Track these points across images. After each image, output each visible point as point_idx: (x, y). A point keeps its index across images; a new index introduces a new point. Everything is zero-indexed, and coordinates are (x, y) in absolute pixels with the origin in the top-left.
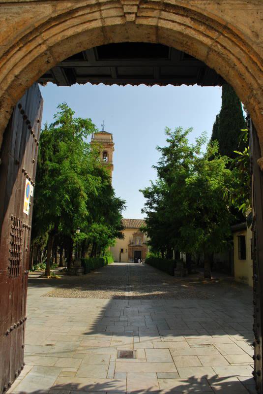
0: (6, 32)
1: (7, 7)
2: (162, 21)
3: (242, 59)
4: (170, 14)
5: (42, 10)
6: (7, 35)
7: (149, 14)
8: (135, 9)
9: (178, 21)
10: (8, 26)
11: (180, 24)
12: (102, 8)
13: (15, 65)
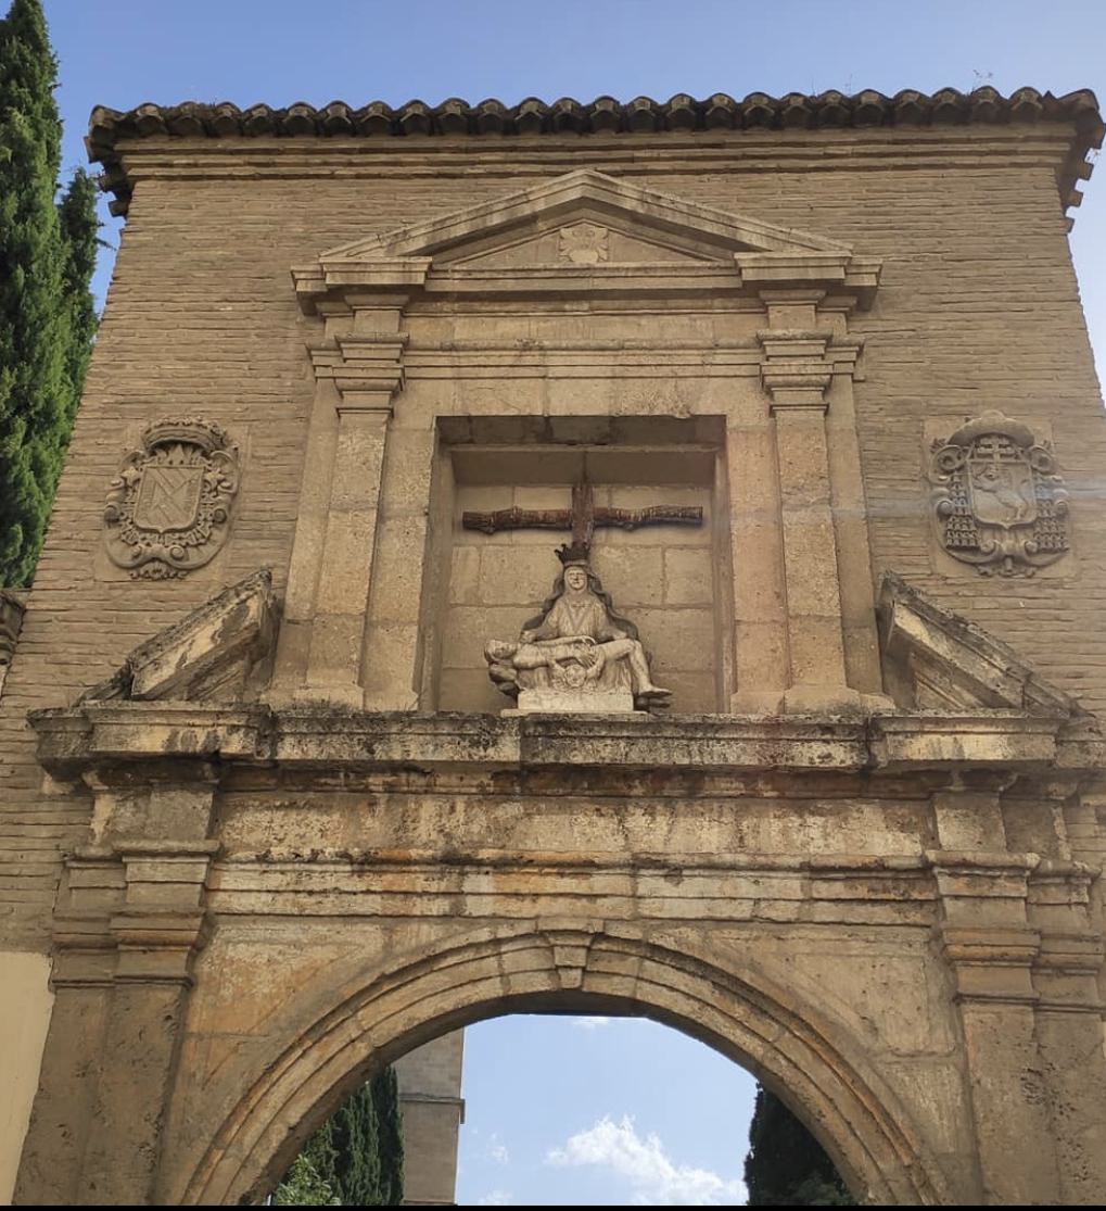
1: (270, 926)
2: (647, 987)
3: (839, 1101)
4: (663, 967)
5: (360, 940)
6: (269, 1007)
8: (580, 957)
9: (682, 988)
10: (273, 981)
11: (689, 996)
12: (504, 949)
13: (291, 1098)
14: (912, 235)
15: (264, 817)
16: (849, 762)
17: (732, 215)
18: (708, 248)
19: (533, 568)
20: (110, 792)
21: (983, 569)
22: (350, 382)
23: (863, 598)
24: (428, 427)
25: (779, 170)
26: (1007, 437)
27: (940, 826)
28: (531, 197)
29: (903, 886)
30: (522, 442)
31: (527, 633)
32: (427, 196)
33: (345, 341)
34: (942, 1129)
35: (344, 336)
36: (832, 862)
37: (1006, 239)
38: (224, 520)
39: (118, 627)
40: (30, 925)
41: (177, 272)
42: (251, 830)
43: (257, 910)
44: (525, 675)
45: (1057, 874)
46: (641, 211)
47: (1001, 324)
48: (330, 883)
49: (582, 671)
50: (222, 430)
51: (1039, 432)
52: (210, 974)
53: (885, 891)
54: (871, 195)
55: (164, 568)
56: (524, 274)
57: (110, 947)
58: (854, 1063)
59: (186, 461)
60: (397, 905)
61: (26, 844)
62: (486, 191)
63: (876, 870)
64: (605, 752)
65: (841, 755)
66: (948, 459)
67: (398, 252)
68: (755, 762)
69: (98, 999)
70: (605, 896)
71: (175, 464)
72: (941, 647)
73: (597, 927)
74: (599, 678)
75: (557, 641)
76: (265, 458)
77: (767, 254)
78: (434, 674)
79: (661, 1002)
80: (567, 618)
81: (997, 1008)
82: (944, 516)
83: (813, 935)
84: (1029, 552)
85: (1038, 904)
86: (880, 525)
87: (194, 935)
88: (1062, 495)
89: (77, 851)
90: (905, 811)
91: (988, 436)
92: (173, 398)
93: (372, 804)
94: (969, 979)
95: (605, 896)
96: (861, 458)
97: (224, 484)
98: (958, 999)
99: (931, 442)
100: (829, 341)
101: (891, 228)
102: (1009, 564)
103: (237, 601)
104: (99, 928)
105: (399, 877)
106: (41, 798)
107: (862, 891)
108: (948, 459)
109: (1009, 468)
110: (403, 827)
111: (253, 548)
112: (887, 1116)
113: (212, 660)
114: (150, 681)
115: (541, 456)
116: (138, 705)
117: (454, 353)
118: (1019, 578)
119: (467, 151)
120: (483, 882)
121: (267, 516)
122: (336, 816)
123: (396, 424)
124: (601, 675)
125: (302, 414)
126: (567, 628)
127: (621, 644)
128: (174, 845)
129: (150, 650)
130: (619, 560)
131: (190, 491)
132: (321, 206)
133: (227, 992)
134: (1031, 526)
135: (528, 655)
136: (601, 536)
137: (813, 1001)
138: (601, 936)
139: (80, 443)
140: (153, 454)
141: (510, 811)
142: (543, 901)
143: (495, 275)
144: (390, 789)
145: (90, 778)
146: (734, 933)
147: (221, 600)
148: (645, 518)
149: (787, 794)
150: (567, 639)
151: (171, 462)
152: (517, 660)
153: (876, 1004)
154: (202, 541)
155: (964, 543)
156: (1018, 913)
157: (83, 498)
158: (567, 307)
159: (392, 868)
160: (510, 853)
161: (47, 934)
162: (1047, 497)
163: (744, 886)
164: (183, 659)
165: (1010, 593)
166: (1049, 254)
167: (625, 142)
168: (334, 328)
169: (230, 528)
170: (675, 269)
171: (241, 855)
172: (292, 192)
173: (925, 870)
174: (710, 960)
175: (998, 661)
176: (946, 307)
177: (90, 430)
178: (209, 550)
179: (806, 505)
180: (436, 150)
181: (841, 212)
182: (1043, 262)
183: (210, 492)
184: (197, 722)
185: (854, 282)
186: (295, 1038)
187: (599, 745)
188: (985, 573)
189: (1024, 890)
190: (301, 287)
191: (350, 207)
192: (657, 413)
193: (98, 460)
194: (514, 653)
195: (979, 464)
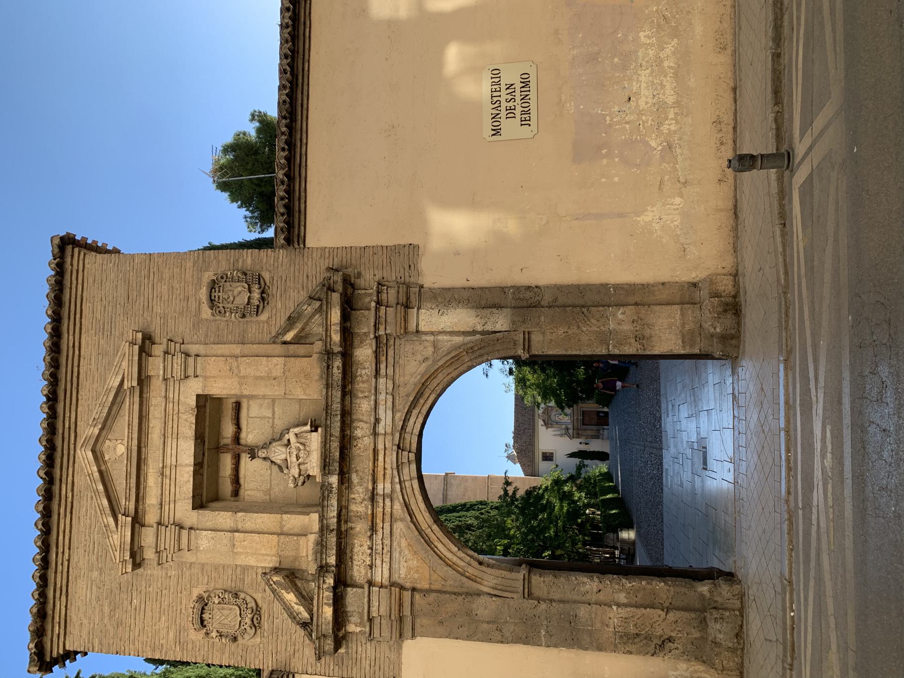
0: (418, 560)
1: (394, 562)
5: (399, 531)
7: (408, 441)
8: (405, 453)
13: (449, 550)
14: (115, 314)
15: (355, 568)
16: (340, 360)
17: (105, 388)
18: (119, 399)
19: (255, 469)
20: (345, 626)
21: (266, 304)
23: (278, 349)
24: (197, 513)
25: (79, 366)
26: (212, 289)
27: (362, 331)
28: (90, 472)
29: (381, 345)
30: (202, 475)
32: (81, 518)
33: (157, 550)
35: (154, 550)
36: (374, 368)
37: (119, 278)
38: (236, 594)
40: (393, 650)
41: (116, 626)
42: (360, 573)
43: (389, 568)
45: (378, 296)
47: (159, 284)
49: (302, 452)
50: (194, 598)
51: (209, 277)
52: (410, 583)
53: (383, 351)
54: (94, 329)
55: (256, 616)
57: (401, 619)
58: (437, 367)
59: (209, 612)
60: (388, 518)
62: (80, 492)
64: (335, 445)
65: (338, 363)
66: (219, 312)
67: (115, 529)
68: (340, 393)
69: (418, 621)
70: (385, 444)
71: (211, 616)
72: (299, 326)
73: (395, 448)
75: (289, 460)
76: (208, 580)
77: (126, 376)
78: (304, 508)
79: (419, 426)
80: (279, 456)
81: (420, 320)
83: (398, 375)
84: (260, 288)
86: (246, 339)
87: (397, 589)
88: (237, 273)
90: (356, 341)
91: (211, 296)
92: (178, 621)
93: (351, 528)
95: (385, 444)
97: (220, 595)
100: (166, 353)
101: (111, 322)
102: (264, 295)
103: (274, 585)
104: (394, 623)
105: (378, 517)
106: (347, 653)
107: (383, 358)
108: (219, 312)
109: (225, 290)
110: (360, 517)
112: (452, 358)
113: (296, 593)
114: (305, 615)
115: (209, 466)
116: (315, 619)
117: (163, 503)
118: (269, 291)
119: (60, 501)
120: (380, 487)
121: (234, 577)
122: (356, 541)
123: (195, 526)
125: (188, 565)
127: (291, 436)
128: (366, 600)
129: (293, 616)
131: (223, 609)
132: (84, 564)
133: (416, 576)
134: (249, 285)
135: (295, 471)
136: (242, 442)
137: (419, 377)
138: (399, 447)
139: (198, 658)
140: (205, 626)
141: (355, 478)
142: (386, 466)
143: (128, 487)
144: (346, 522)
146: (397, 401)
147: (274, 591)
148: (236, 425)
149: (350, 380)
150: (288, 456)
151: (210, 618)
152: (297, 476)
153: (419, 357)
154: (245, 602)
155: (255, 310)
157: (223, 653)
158: (143, 457)
159: (375, 520)
160: (370, 478)
163: (382, 397)
164: (297, 604)
165: (275, 295)
166: (128, 262)
167: (61, 431)
168: (149, 554)
169: (240, 591)
170: (129, 413)
171: (369, 575)
172: (76, 578)
173: (377, 338)
174: (406, 410)
175: (305, 307)
176: (150, 304)
177: (192, 655)
178: (249, 599)
179: (238, 367)
180: (59, 514)
181: (102, 342)
182: (132, 264)
183: (223, 601)
184: (321, 596)
185: (139, 341)
186: (431, 551)
188: (268, 304)
189: (383, 308)
190: (129, 569)
191: (85, 551)
192: (194, 421)
193: (206, 649)
194: (294, 477)
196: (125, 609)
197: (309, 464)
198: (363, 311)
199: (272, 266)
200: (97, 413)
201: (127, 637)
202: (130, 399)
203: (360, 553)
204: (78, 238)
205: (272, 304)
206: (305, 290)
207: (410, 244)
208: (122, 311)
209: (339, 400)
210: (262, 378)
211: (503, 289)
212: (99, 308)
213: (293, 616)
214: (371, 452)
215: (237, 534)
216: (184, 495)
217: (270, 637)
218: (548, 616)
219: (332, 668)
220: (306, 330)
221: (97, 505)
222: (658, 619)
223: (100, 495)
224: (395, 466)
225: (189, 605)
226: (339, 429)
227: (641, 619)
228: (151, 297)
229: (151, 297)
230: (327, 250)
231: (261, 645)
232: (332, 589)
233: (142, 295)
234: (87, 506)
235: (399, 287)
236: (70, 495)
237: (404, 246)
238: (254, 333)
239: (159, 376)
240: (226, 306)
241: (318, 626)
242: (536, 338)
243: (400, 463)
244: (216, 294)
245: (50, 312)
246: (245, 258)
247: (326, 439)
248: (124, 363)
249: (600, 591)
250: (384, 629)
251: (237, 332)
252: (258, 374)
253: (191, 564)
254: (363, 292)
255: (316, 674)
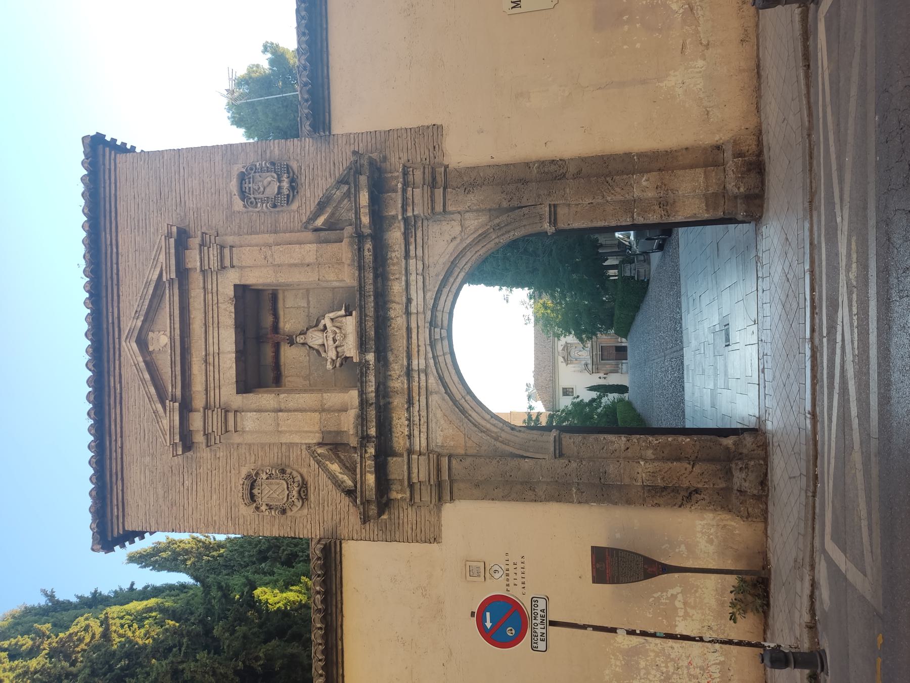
3: (476, 250)
5: (434, 403)
7: (439, 319)
8: (438, 330)
11: (448, 296)
13: (483, 418)
14: (149, 211)
15: (395, 439)
17: (145, 282)
18: (158, 292)
19: (294, 356)
21: (295, 193)
22: (223, 428)
23: (310, 235)
24: (241, 397)
25: (117, 264)
27: (390, 214)
28: (136, 363)
29: (410, 227)
31: (323, 355)
32: (131, 407)
33: (205, 432)
34: (483, 219)
35: (202, 433)
36: (403, 249)
39: (326, 503)
40: (432, 513)
41: (170, 506)
42: (399, 443)
44: (340, 355)
45: (404, 178)
46: (142, 318)
47: (190, 179)
48: (416, 414)
51: (238, 169)
53: (412, 232)
54: (129, 227)
55: (303, 489)
56: (173, 364)
57: (440, 484)
59: (258, 487)
60: (423, 392)
61: (406, 520)
63: (406, 236)
64: (370, 324)
65: (368, 245)
68: (372, 274)
70: (417, 323)
71: (260, 491)
72: (329, 210)
74: (340, 328)
76: (255, 459)
77: (164, 268)
80: (317, 342)
81: (447, 200)
82: (275, 206)
83: (427, 256)
84: (288, 177)
85: (414, 184)
88: (265, 164)
89: (408, 500)
91: (241, 188)
94: (439, 208)
95: (417, 323)
96: (251, 235)
97: (268, 471)
98: (444, 210)
99: (244, 209)
100: (202, 245)
101: (146, 219)
102: (294, 184)
104: (434, 488)
107: (412, 240)
109: (256, 180)
111: (293, 458)
112: (480, 235)
114: (349, 483)
120: (415, 363)
121: (280, 455)
122: (394, 415)
124: (339, 328)
125: (235, 446)
126: (320, 342)
127: (327, 321)
128: (406, 467)
130: (290, 324)
131: (271, 484)
132: (136, 451)
134: (278, 175)
135: (332, 354)
136: (281, 331)
140: (255, 501)
143: (174, 375)
144: (384, 397)
145: (384, 500)
146: (427, 281)
147: (318, 462)
148: (273, 314)
150: (325, 341)
152: (334, 358)
153: (447, 237)
155: (286, 199)
156: (418, 191)
157: (273, 525)
158: (186, 346)
161: (435, 507)
162: (266, 169)
163: (413, 278)
165: (304, 184)
166: (157, 159)
168: (199, 438)
170: (170, 304)
171: (408, 444)
172: (130, 464)
173: (406, 220)
174: (436, 289)
175: (333, 192)
176: (182, 199)
178: (295, 474)
180: (109, 405)
182: (161, 161)
187: (368, 326)
188: (297, 192)
190: (180, 451)
192: (233, 310)
193: (257, 522)
194: (332, 359)
195: (253, 192)
196: (177, 490)
197: (345, 346)
198: (390, 194)
199: (299, 155)
200: (138, 306)
201: (182, 515)
202: (169, 291)
203: (399, 426)
204: (108, 138)
205: (302, 192)
206: (332, 177)
207: (434, 125)
208: (155, 208)
209: (371, 281)
210: (295, 265)
211: (528, 165)
212: (133, 205)
213: (338, 484)
214: (405, 330)
215: (280, 414)
216: (228, 381)
217: (317, 508)
218: (579, 474)
219: (376, 533)
220: (336, 215)
221: (144, 393)
222: (685, 472)
223: (147, 383)
224: (428, 342)
225: (238, 483)
226: (373, 309)
227: (669, 472)
228: (182, 192)
229: (182, 192)
230: (352, 136)
231: (309, 516)
232: (373, 458)
233: (174, 190)
234: (135, 397)
235: (424, 168)
236: (118, 386)
237: (428, 127)
238: (286, 223)
239: (196, 269)
240: (257, 196)
241: (362, 492)
242: (562, 212)
243: (433, 339)
244: (246, 185)
245: (86, 211)
246: (272, 148)
247: (361, 319)
248: (161, 256)
249: (628, 448)
250: (425, 495)
251: (269, 222)
252: (292, 261)
253: (238, 445)
254: (389, 175)
255: (361, 540)
